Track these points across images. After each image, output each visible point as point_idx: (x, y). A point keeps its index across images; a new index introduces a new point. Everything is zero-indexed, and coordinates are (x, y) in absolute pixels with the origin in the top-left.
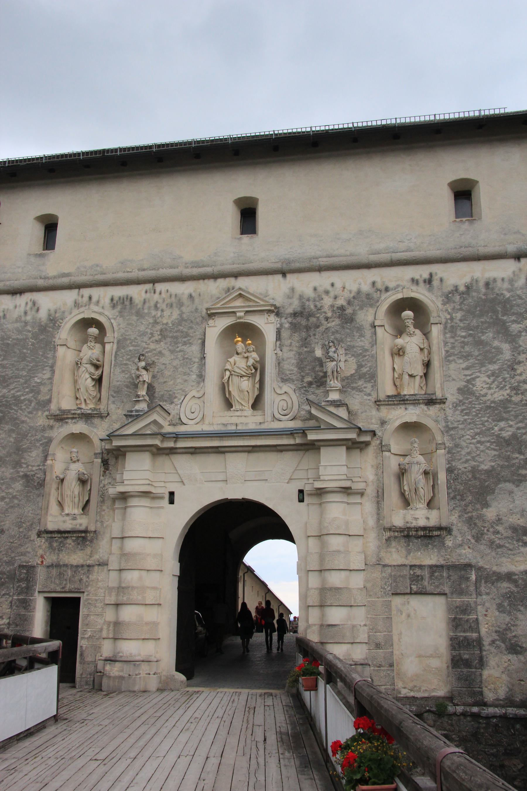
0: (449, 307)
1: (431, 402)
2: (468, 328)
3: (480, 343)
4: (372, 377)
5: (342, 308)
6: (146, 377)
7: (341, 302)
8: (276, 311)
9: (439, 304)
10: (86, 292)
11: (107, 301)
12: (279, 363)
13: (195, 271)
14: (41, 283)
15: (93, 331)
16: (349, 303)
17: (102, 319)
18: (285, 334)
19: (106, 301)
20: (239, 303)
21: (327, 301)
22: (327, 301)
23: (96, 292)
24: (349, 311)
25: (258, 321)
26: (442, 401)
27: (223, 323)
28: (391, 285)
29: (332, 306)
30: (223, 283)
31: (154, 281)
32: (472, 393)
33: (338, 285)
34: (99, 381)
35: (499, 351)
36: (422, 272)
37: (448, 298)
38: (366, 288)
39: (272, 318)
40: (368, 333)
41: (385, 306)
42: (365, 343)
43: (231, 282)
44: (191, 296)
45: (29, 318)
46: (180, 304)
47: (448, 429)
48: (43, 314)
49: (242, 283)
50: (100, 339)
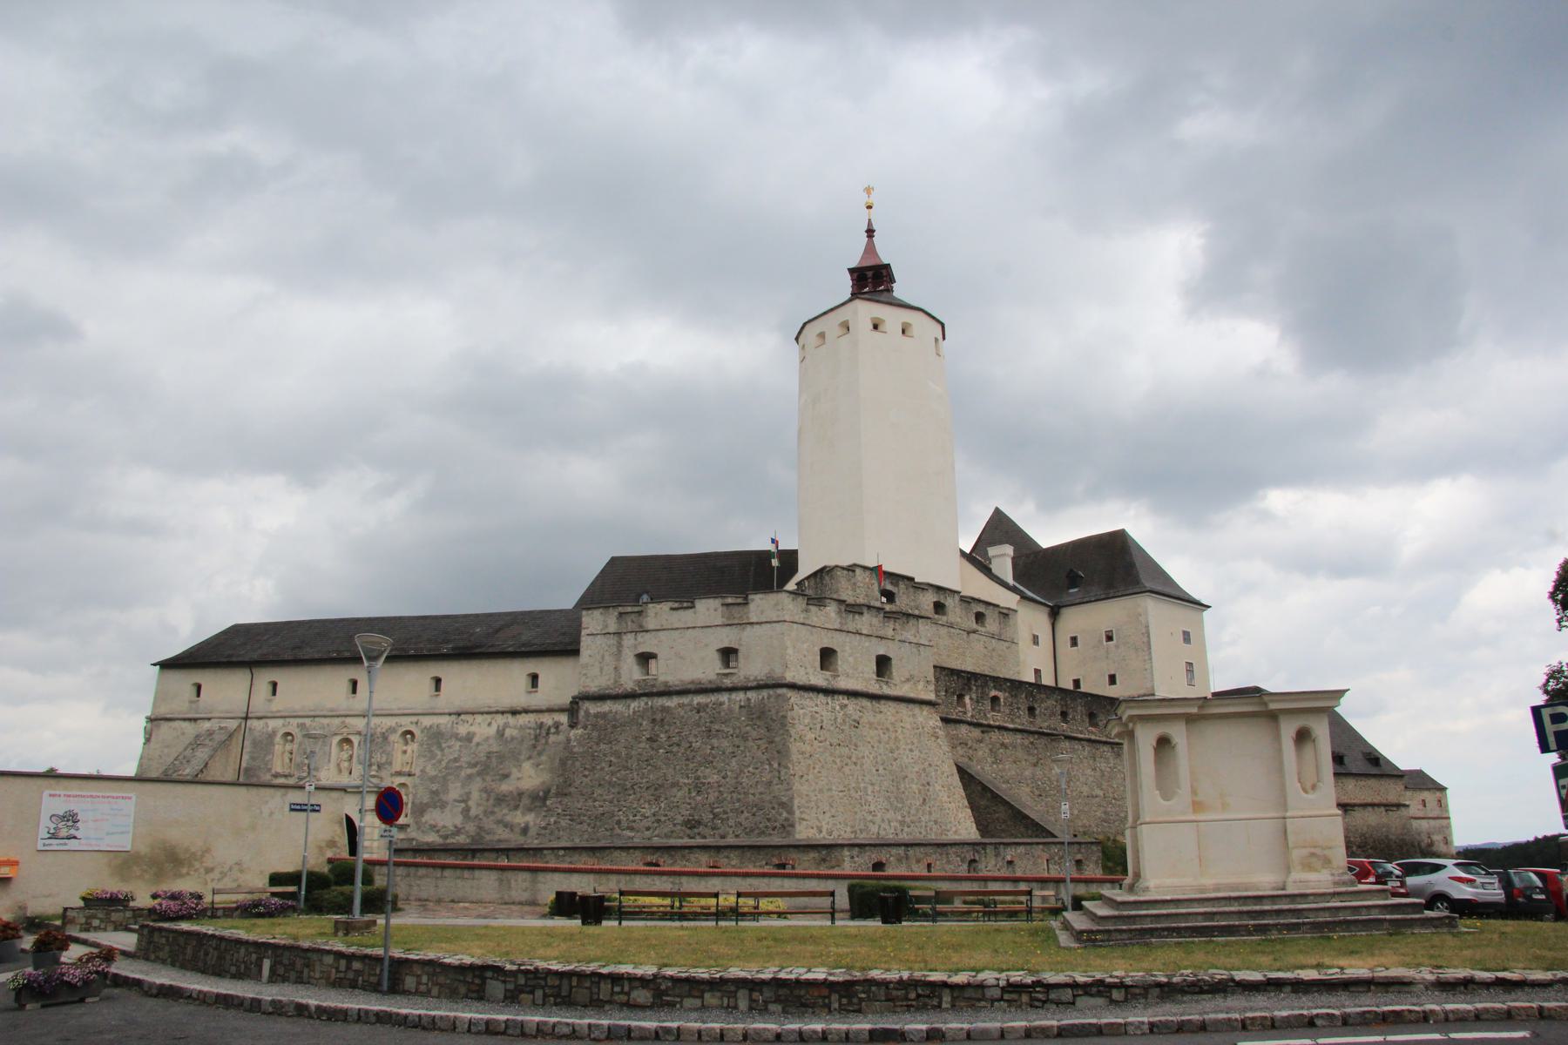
0: (423, 735)
1: (410, 775)
2: (428, 744)
3: (431, 751)
4: (391, 764)
5: (384, 733)
6: (306, 761)
7: (384, 730)
8: (359, 733)
10: (288, 720)
11: (296, 725)
12: (358, 757)
13: (330, 714)
14: (269, 715)
15: (290, 738)
16: (387, 731)
17: (294, 733)
20: (345, 730)
22: (379, 730)
23: (291, 720)
24: (386, 734)
25: (350, 737)
26: (414, 775)
27: (338, 738)
28: (403, 724)
30: (340, 719)
31: (314, 717)
32: (425, 772)
33: (384, 722)
34: (291, 760)
35: (437, 755)
36: (414, 719)
37: (422, 732)
38: (394, 725)
39: (358, 737)
41: (400, 732)
42: (389, 749)
43: (343, 719)
44: (328, 725)
45: (265, 730)
46: (324, 728)
47: (415, 786)
49: (348, 720)
50: (292, 741)
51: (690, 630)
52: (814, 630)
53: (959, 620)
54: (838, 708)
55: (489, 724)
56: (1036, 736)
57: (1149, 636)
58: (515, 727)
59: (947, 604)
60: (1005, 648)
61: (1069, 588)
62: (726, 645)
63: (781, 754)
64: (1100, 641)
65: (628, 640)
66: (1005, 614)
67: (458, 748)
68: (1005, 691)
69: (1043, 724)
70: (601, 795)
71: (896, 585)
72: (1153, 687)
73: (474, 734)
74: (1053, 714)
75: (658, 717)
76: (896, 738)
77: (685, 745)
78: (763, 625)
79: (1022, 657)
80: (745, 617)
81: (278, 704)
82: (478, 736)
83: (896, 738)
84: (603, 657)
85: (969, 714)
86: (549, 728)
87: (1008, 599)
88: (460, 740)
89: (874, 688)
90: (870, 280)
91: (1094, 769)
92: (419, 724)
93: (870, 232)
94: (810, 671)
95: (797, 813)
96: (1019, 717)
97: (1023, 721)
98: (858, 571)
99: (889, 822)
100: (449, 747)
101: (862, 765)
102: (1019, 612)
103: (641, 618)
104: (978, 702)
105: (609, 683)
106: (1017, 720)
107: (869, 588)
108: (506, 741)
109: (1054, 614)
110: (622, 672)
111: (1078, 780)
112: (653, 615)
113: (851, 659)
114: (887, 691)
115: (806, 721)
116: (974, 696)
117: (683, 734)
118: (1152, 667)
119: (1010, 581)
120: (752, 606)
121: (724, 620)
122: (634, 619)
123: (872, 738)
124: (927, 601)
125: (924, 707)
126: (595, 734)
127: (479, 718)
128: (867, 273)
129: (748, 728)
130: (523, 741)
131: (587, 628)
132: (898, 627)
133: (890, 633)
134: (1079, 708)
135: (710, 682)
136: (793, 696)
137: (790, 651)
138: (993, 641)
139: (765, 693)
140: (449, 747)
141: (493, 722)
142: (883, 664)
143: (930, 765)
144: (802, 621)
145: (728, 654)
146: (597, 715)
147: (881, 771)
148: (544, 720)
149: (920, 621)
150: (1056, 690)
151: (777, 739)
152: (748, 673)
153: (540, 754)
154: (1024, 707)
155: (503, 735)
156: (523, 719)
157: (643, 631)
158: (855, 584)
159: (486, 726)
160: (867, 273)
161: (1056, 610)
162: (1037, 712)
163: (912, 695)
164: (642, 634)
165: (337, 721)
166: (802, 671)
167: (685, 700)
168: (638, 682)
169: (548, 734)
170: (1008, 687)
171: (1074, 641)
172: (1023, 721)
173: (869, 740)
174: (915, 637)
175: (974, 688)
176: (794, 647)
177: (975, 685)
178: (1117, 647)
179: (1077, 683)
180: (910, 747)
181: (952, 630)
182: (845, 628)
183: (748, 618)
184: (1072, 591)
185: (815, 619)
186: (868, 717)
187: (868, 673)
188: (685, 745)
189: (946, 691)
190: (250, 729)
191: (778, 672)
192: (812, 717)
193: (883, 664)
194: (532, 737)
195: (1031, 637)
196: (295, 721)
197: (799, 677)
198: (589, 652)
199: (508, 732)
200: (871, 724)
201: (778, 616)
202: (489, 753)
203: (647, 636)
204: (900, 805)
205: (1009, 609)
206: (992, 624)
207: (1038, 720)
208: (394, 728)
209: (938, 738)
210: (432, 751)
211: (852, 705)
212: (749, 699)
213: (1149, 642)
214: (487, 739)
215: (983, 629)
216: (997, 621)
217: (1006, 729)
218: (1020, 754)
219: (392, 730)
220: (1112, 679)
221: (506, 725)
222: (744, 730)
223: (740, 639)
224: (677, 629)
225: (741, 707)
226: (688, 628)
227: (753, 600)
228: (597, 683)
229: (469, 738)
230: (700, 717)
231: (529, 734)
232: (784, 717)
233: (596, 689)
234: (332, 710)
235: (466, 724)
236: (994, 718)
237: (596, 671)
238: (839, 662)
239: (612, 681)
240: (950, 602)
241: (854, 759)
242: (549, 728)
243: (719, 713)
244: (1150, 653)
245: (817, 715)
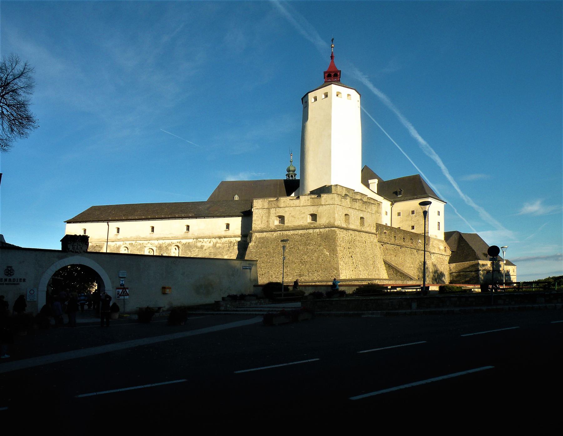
3: (186, 252)
5: (166, 246)
7: (166, 245)
9: (181, 246)
18: (157, 250)
19: (128, 244)
21: (164, 245)
22: (164, 245)
24: (167, 247)
28: (174, 243)
29: (165, 246)
35: (189, 254)
36: (179, 241)
37: (182, 245)
38: (170, 243)
40: (170, 250)
48: (118, 246)
49: (151, 241)
54: (349, 235)
55: (210, 242)
58: (220, 243)
63: (333, 251)
65: (273, 211)
67: (197, 251)
69: (397, 242)
70: (264, 266)
73: (204, 246)
77: (296, 248)
78: (327, 206)
81: (120, 236)
82: (205, 247)
83: (366, 246)
84: (262, 217)
86: (234, 243)
88: (198, 248)
89: (359, 228)
91: (411, 258)
92: (181, 242)
94: (342, 222)
95: (340, 272)
97: (393, 241)
99: (365, 274)
100: (194, 251)
101: (357, 255)
105: (265, 226)
108: (217, 248)
110: (270, 222)
111: (407, 261)
121: (311, 204)
126: (260, 245)
127: (206, 240)
130: (224, 248)
131: (256, 207)
135: (305, 226)
137: (336, 215)
140: (194, 251)
141: (211, 242)
143: (375, 255)
146: (260, 238)
147: (362, 257)
148: (232, 241)
151: (332, 246)
152: (320, 223)
153: (231, 253)
154: (393, 236)
155: (216, 246)
156: (224, 240)
159: (208, 243)
165: (147, 242)
167: (296, 232)
168: (276, 226)
169: (234, 246)
172: (393, 241)
176: (338, 214)
180: (369, 249)
185: (343, 204)
188: (296, 248)
190: (109, 246)
191: (332, 221)
192: (343, 238)
194: (228, 247)
196: (128, 242)
197: (337, 223)
198: (256, 215)
199: (218, 245)
200: (359, 240)
202: (210, 253)
204: (367, 269)
207: (396, 241)
208: (170, 244)
210: (187, 253)
212: (321, 232)
214: (209, 247)
218: (392, 252)
219: (170, 245)
221: (217, 243)
225: (318, 235)
227: (323, 197)
228: (260, 226)
229: (202, 247)
231: (226, 246)
232: (335, 238)
233: (260, 229)
234: (144, 238)
235: (200, 242)
237: (260, 222)
239: (266, 226)
241: (355, 253)
242: (234, 243)
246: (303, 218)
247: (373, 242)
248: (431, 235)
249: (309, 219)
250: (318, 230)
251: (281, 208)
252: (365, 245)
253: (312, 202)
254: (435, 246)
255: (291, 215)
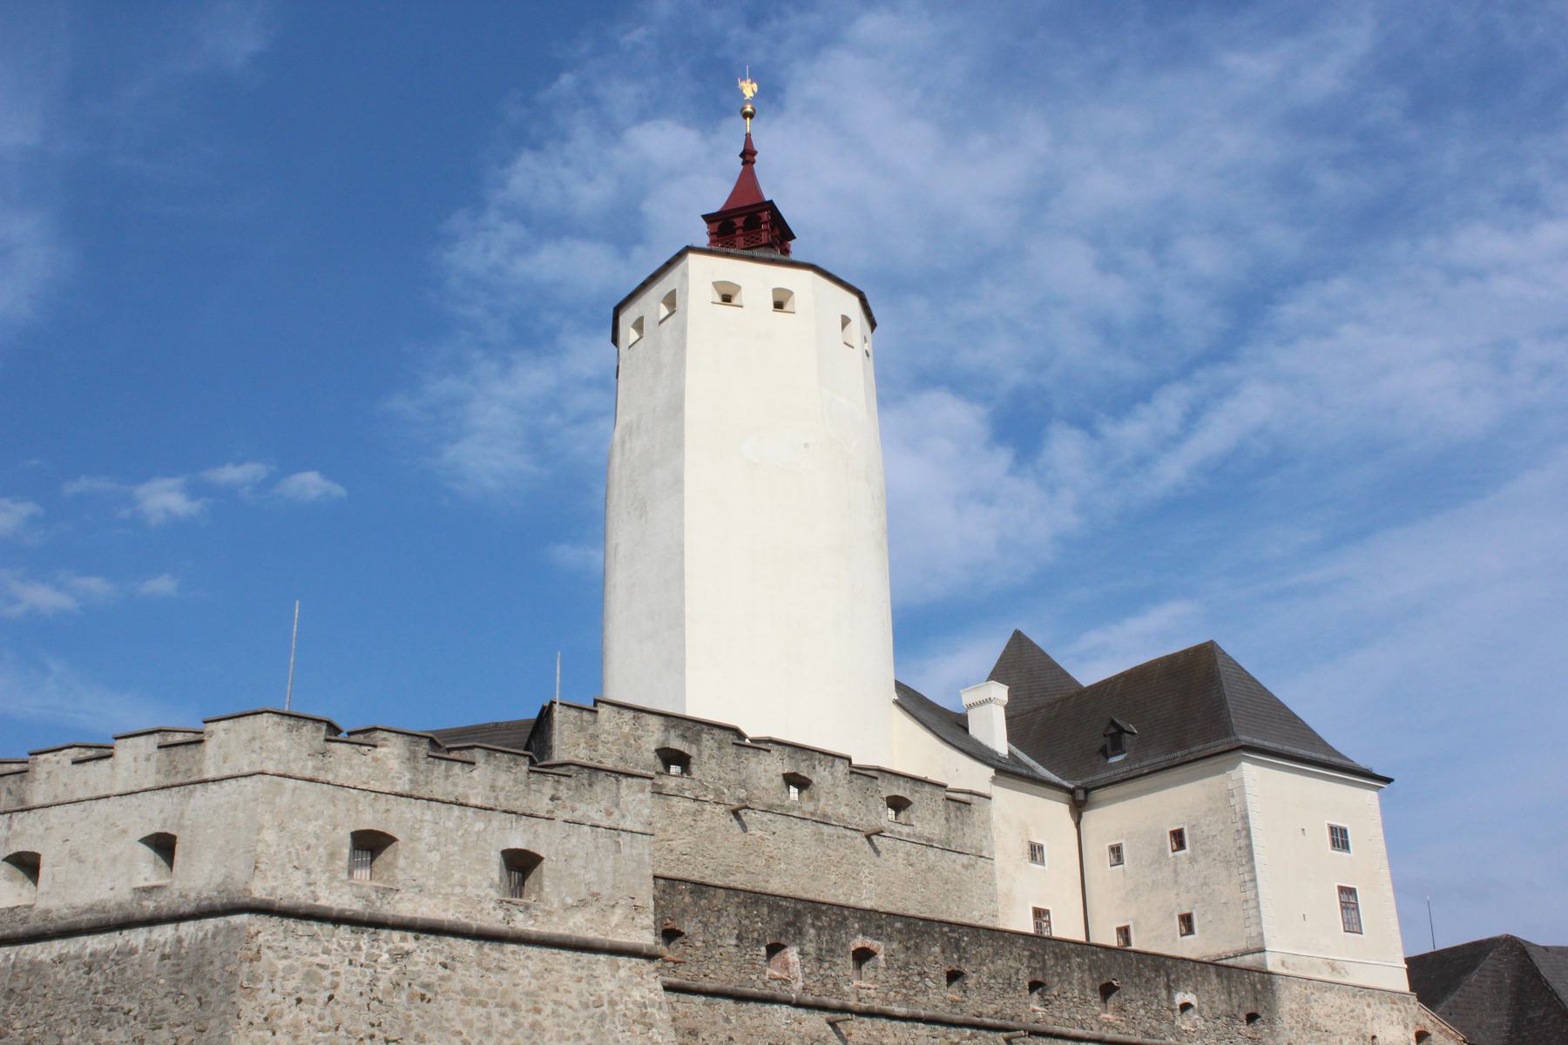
51: (101, 801)
52: (341, 793)
53: (845, 810)
54: (385, 957)
56: (968, 1032)
57: (1248, 836)
59: (815, 779)
60: (959, 868)
61: (1107, 758)
62: (157, 828)
64: (1162, 852)
66: (961, 803)
68: (890, 938)
69: (976, 1004)
71: (696, 740)
72: (1261, 935)
74: (1010, 985)
75: (20, 985)
76: (534, 1026)
78: (224, 783)
79: (1001, 885)
80: (195, 770)
85: (798, 986)
87: (975, 776)
89: (492, 919)
90: (739, 232)
93: (748, 155)
96: (925, 992)
97: (938, 997)
98: (604, 711)
102: (994, 804)
103: (24, 785)
104: (820, 960)
106: (921, 999)
107: (627, 744)
109: (1078, 807)
112: (44, 775)
113: (435, 857)
114: (522, 923)
115: (290, 985)
116: (810, 948)
117: (52, 1019)
118: (1257, 896)
119: (1000, 743)
120: (210, 747)
122: (13, 787)
123: (469, 1024)
124: (773, 767)
125: (622, 960)
128: (735, 220)
129: (167, 1001)
132: (563, 792)
133: (542, 805)
134: (1077, 975)
136: (266, 930)
138: (930, 852)
139: (210, 924)
142: (521, 864)
144: (308, 774)
145: (163, 845)
149: (624, 781)
150: (1086, 948)
154: (938, 972)
157: (22, 810)
158: (595, 737)
160: (735, 220)
161: (1080, 795)
162: (971, 983)
163: (591, 934)
164: (21, 815)
166: (298, 878)
170: (900, 931)
171: (1116, 851)
172: (938, 997)
173: (459, 1027)
174: (609, 814)
175: (812, 931)
177: (813, 925)
178: (1193, 860)
179: (1124, 932)
181: (825, 829)
182: (423, 792)
183: (200, 771)
184: (1113, 760)
186: (465, 976)
187: (477, 887)
189: (739, 937)
191: (240, 875)
192: (309, 976)
193: (521, 864)
195: (1027, 847)
201: (252, 763)
203: (29, 818)
205: (971, 793)
206: (927, 819)
209: (650, 1026)
211: (424, 952)
213: (1249, 846)
215: (906, 830)
216: (941, 815)
217: (892, 1017)
220: (1187, 921)
222: (159, 1005)
223: (182, 815)
224: (79, 801)
225: (164, 957)
226: (98, 798)
230: (91, 981)
236: (863, 987)
238: (401, 862)
240: (821, 775)
243: (123, 970)
244: (1253, 869)
245: (324, 973)
246: (114, 860)
247: (612, 1003)
248: (1290, 960)
249: (146, 869)
250: (165, 933)
251: (32, 813)
252: (531, 1018)
253: (163, 770)
254: (1329, 1024)
255: (68, 846)
